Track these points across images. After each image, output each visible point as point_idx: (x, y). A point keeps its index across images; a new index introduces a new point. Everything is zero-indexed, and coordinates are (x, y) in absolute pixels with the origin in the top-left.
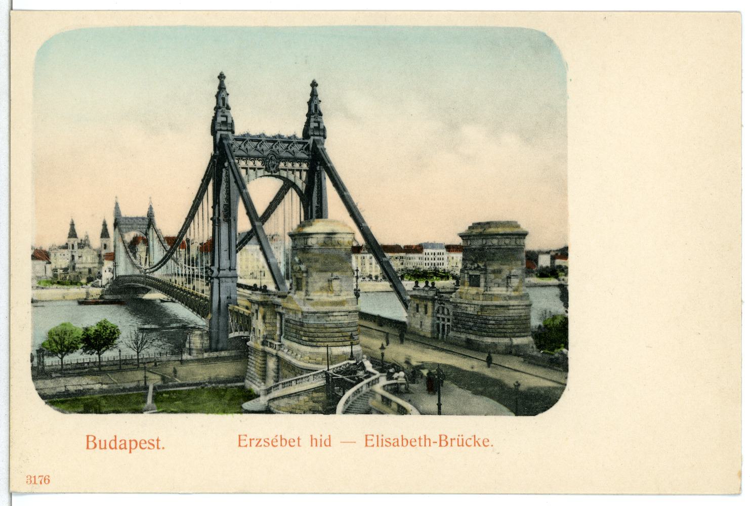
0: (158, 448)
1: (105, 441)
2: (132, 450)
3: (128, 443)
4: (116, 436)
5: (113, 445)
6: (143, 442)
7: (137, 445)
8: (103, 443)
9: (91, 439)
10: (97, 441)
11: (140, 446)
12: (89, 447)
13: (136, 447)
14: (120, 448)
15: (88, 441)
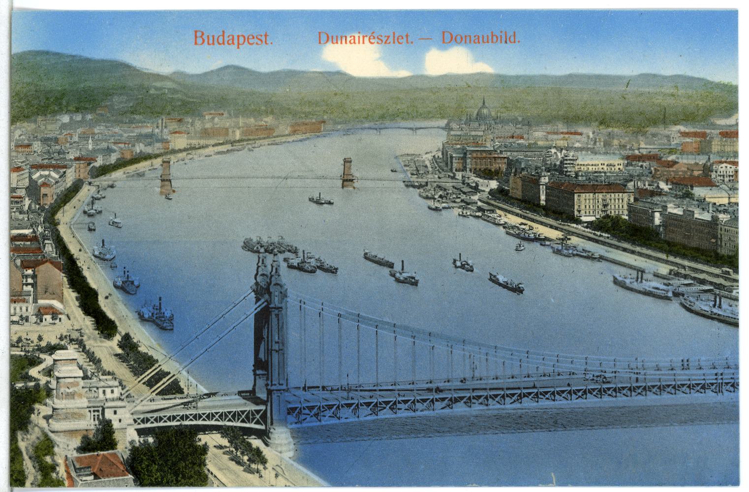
0: (266, 43)
1: (213, 37)
2: (240, 46)
3: (236, 38)
5: (221, 41)
8: (211, 39)
9: (199, 34)
10: (205, 37)
11: (248, 41)
13: (243, 43)
14: (229, 44)
15: (196, 37)
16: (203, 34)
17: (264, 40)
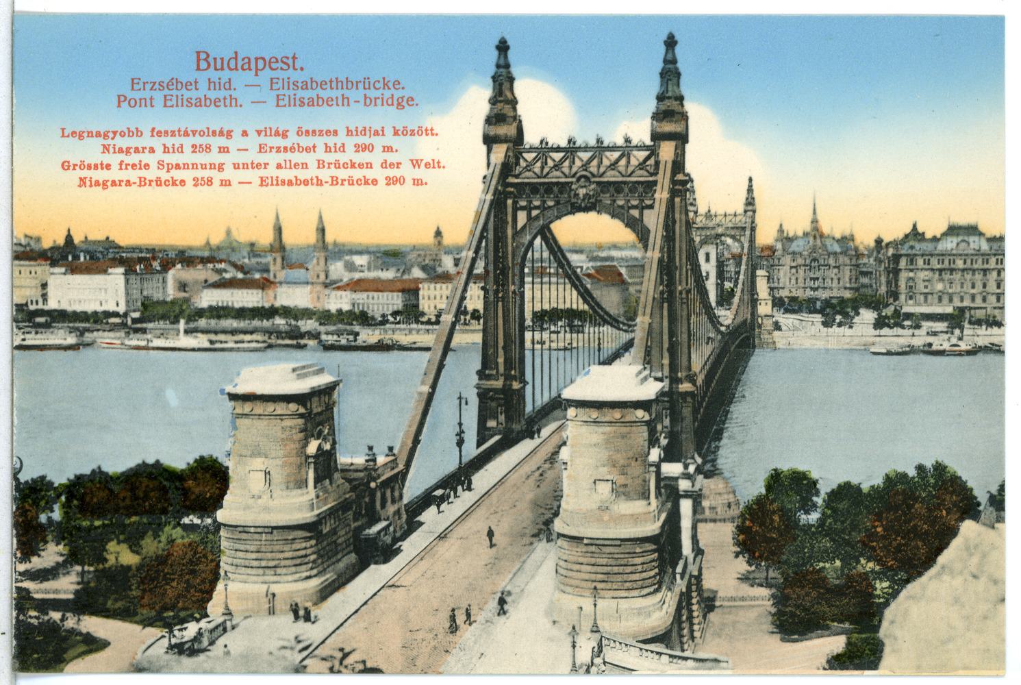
0: (295, 69)
1: (222, 59)
2: (259, 72)
3: (253, 62)
4: (236, 53)
5: (232, 65)
9: (203, 56)
10: (211, 60)
12: (201, 68)
13: (264, 68)
14: (243, 69)
17: (291, 64)
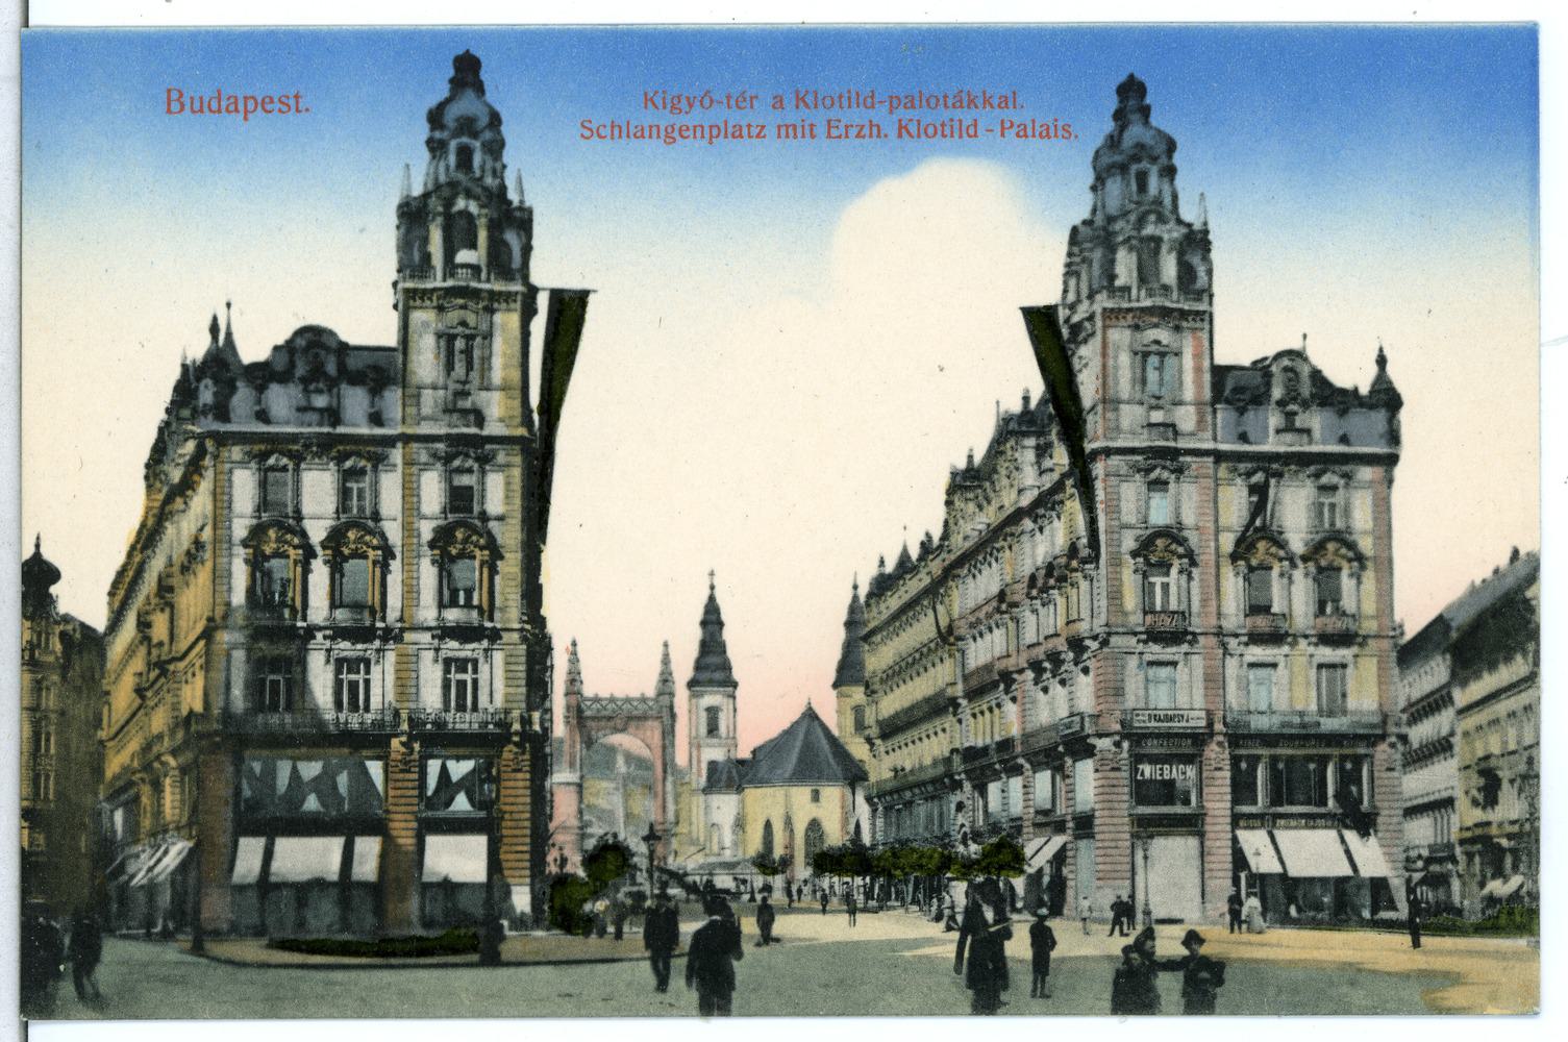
0: (297, 110)
1: (201, 98)
5: (214, 106)
6: (267, 100)
7: (256, 107)
9: (175, 95)
10: (186, 100)
12: (173, 109)
13: (255, 110)
16: (181, 95)
